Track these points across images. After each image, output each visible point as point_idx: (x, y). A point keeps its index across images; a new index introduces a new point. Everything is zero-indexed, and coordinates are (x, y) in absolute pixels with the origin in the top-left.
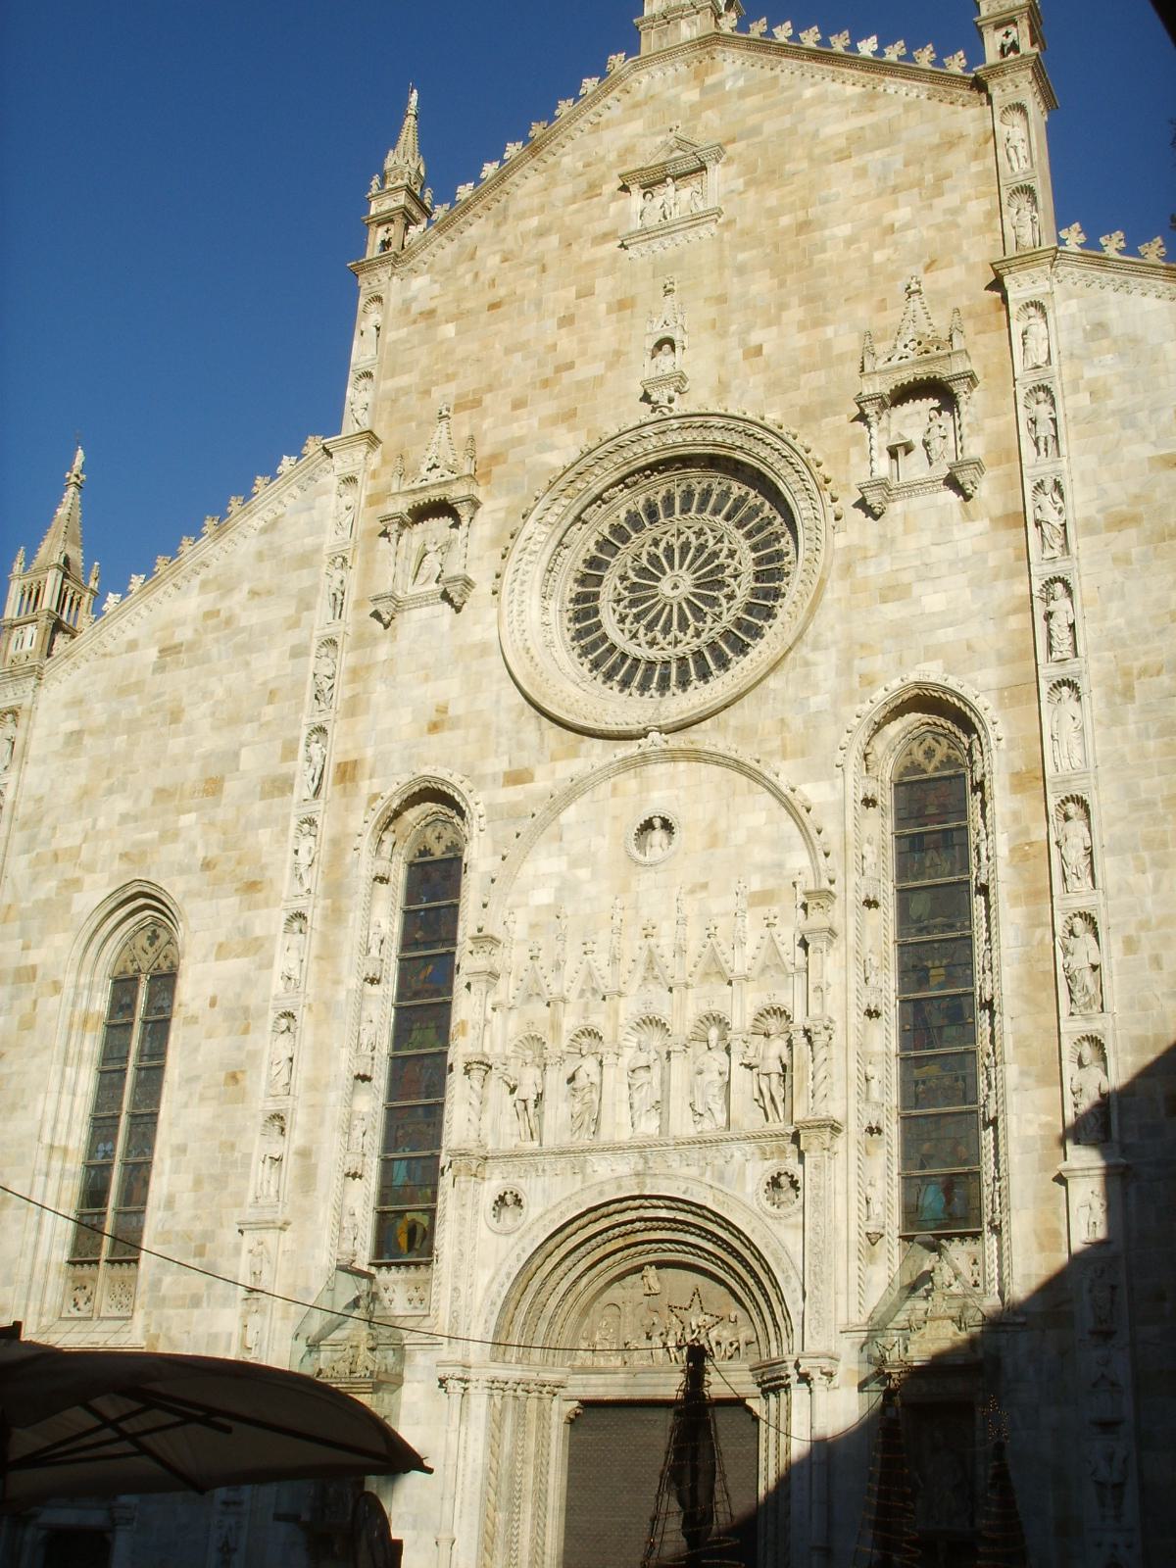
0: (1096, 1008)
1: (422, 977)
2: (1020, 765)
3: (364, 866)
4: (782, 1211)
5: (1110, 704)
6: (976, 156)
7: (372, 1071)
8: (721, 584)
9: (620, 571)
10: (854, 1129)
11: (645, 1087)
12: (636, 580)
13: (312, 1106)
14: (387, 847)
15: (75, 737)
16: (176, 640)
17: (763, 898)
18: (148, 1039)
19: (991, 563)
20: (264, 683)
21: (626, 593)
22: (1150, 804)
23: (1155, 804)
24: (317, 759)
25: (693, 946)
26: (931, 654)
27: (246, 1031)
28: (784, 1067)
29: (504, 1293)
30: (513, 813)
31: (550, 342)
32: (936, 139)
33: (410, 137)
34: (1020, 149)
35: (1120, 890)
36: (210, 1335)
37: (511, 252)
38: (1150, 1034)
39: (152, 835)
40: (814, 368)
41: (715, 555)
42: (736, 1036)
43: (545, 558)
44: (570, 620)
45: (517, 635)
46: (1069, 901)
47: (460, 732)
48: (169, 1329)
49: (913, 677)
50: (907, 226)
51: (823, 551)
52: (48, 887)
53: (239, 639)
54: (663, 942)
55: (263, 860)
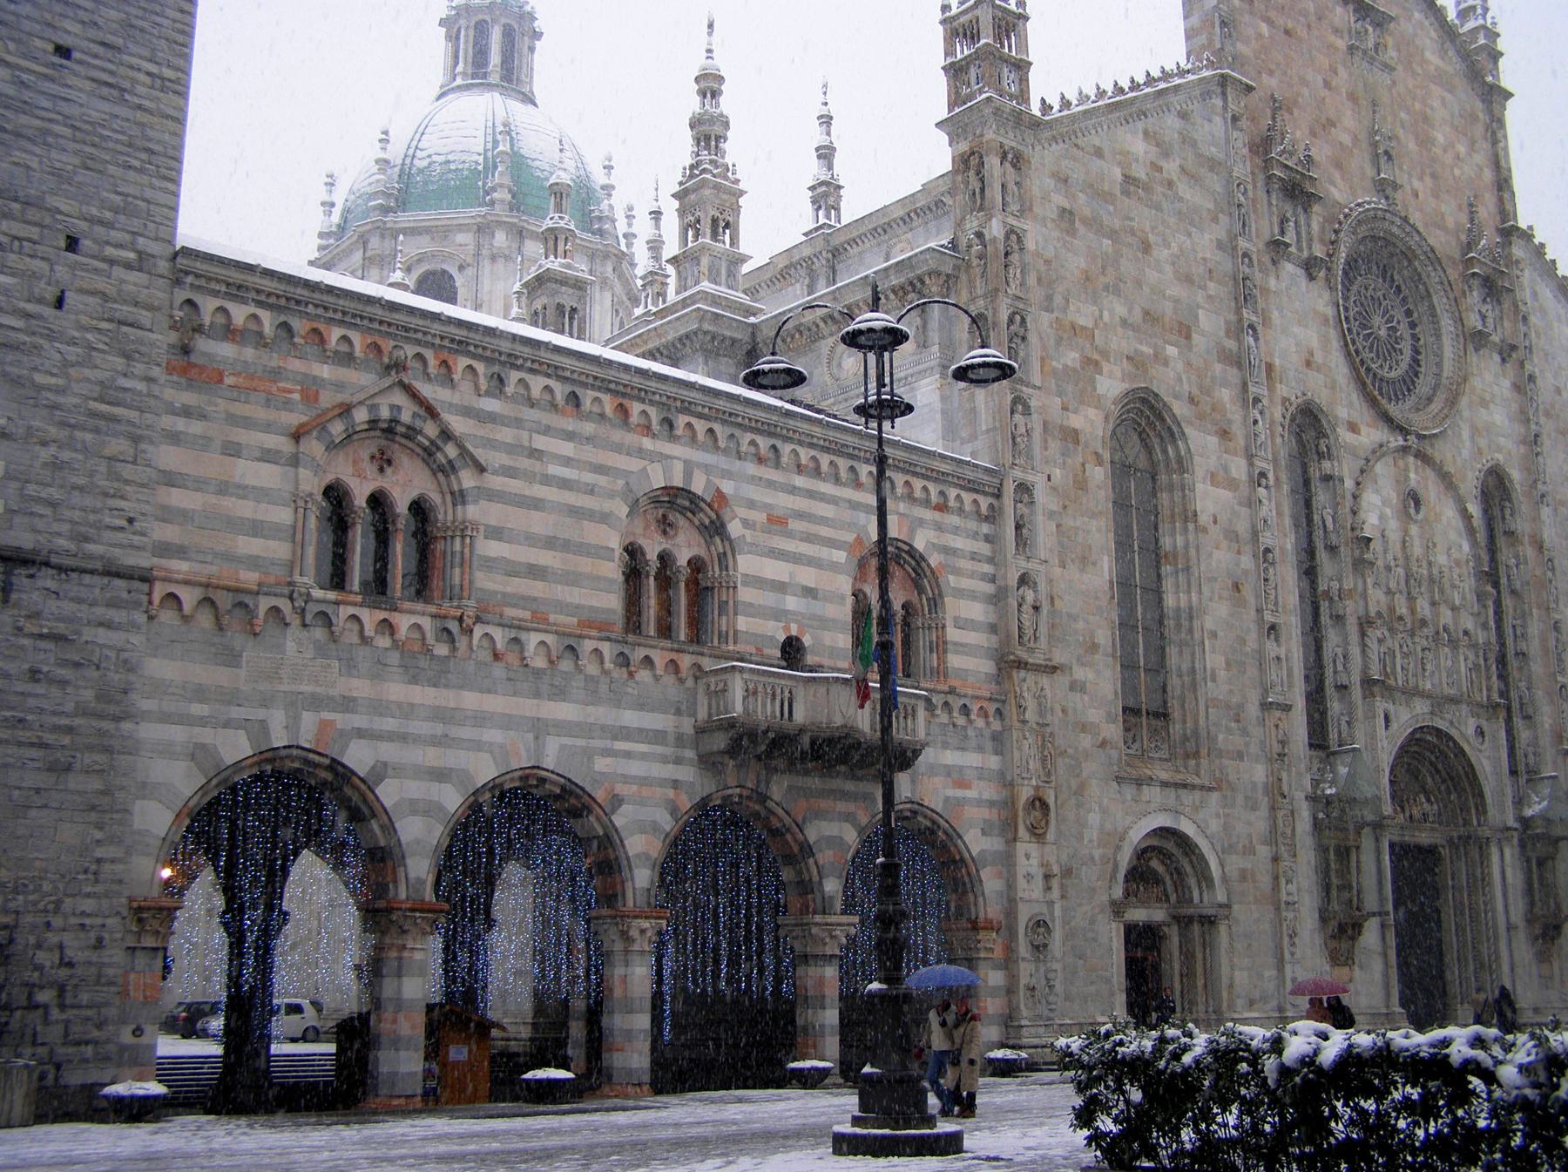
15: (1066, 215)
17: (1458, 563)
20: (1204, 259)
27: (1239, 552)
52: (1071, 358)
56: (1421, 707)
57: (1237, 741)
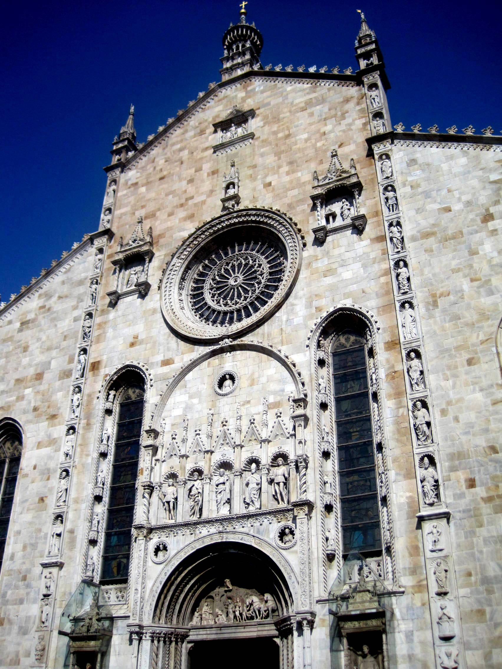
0: (430, 441)
1: (126, 452)
2: (388, 339)
3: (100, 405)
4: (288, 545)
5: (428, 310)
6: (358, 104)
7: (102, 494)
8: (256, 278)
9: (212, 277)
10: (319, 507)
11: (223, 492)
12: (219, 280)
13: (76, 510)
14: (111, 397)
16: (28, 319)
17: (277, 405)
18: (8, 487)
19: (371, 257)
20: (62, 333)
21: (215, 286)
22: (448, 350)
23: (451, 350)
24: (83, 361)
25: (245, 429)
26: (346, 296)
27: (48, 479)
28: (286, 479)
29: (159, 591)
30: (164, 378)
31: (184, 189)
32: (342, 100)
33: (131, 122)
34: (376, 99)
35: (437, 389)
36: (26, 617)
37: (169, 158)
38: (456, 452)
39: (14, 398)
40: (293, 188)
41: (252, 267)
42: (264, 467)
43: (181, 273)
44: (191, 298)
45: (168, 304)
46: (414, 395)
47: (144, 346)
48: (9, 615)
49: (339, 306)
50: (330, 132)
51: (298, 259)
53: (55, 315)
54: (230, 428)
55: (59, 405)
56: (204, 531)
57: (22, 592)
